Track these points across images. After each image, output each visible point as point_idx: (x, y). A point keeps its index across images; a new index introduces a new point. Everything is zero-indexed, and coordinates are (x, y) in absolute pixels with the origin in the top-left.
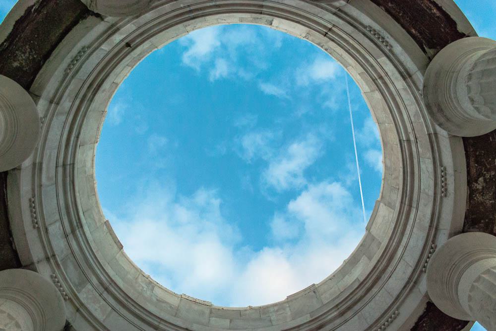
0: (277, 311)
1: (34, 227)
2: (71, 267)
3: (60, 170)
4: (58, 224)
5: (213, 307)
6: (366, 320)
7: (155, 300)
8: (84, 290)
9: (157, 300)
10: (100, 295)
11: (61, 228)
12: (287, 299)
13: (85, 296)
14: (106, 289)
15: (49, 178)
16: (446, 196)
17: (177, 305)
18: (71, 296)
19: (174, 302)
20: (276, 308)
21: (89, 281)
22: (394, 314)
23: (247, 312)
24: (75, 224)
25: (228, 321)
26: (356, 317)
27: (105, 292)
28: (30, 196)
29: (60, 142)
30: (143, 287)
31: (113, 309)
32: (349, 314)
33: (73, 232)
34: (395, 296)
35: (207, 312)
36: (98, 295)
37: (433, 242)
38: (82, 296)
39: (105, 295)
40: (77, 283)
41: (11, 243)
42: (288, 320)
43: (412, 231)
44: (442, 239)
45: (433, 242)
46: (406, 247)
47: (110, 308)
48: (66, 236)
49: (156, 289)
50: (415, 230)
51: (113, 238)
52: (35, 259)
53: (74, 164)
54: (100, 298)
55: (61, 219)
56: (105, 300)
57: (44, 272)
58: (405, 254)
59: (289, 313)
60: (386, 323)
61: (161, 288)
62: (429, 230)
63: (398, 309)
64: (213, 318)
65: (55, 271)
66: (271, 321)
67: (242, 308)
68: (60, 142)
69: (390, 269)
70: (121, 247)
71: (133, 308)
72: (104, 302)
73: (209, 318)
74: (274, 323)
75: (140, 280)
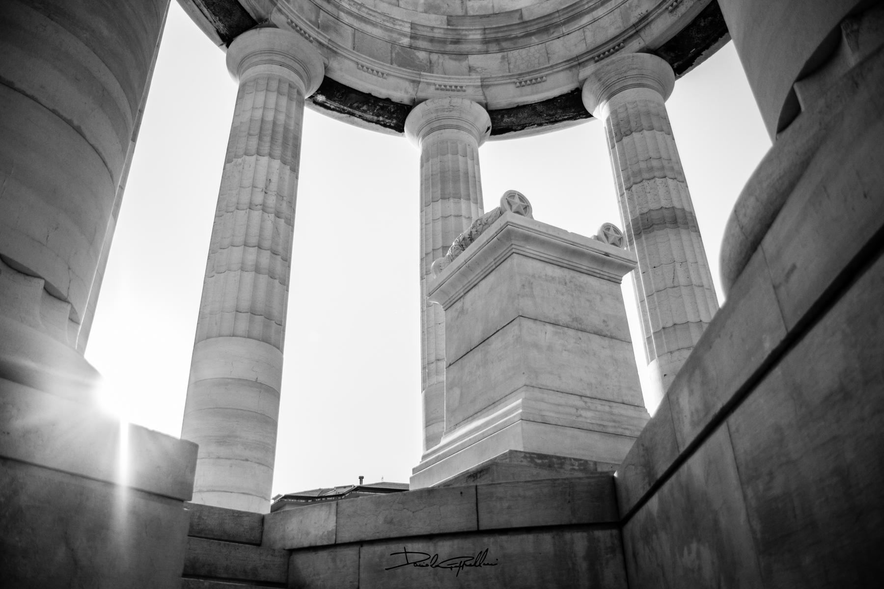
6: (509, 64)
16: (671, 12)
22: (542, 78)
26: (500, 55)
32: (493, 47)
34: (552, 63)
37: (624, 41)
42: (420, 9)
43: (612, 11)
44: (636, 44)
45: (624, 41)
46: (595, 20)
50: (617, 11)
58: (589, 27)
60: (528, 82)
62: (631, 27)
63: (546, 76)
69: (564, 29)
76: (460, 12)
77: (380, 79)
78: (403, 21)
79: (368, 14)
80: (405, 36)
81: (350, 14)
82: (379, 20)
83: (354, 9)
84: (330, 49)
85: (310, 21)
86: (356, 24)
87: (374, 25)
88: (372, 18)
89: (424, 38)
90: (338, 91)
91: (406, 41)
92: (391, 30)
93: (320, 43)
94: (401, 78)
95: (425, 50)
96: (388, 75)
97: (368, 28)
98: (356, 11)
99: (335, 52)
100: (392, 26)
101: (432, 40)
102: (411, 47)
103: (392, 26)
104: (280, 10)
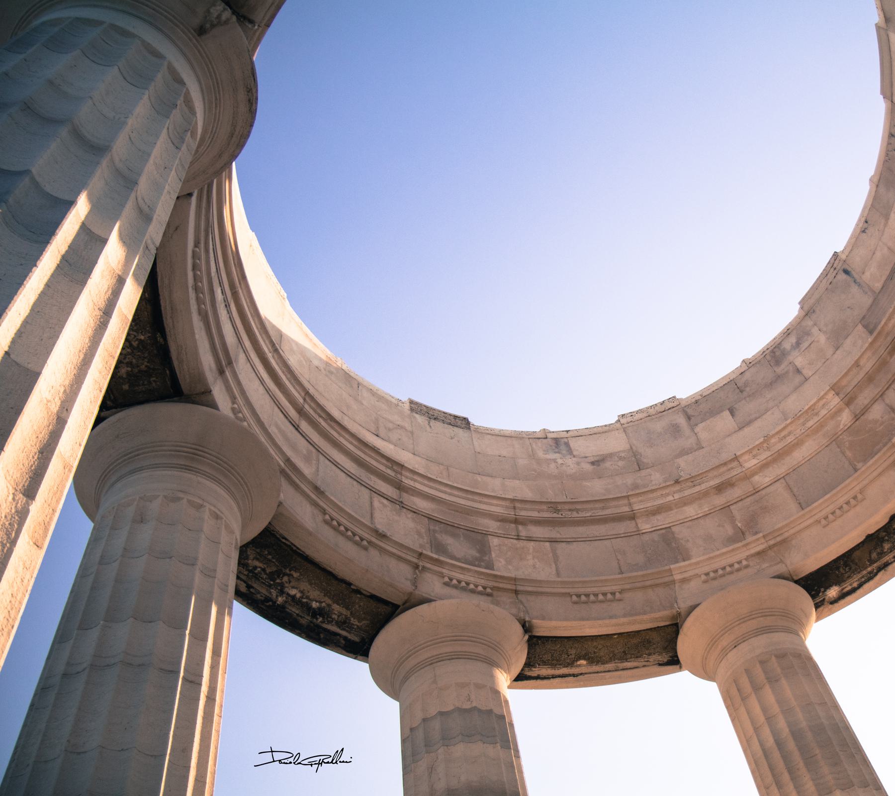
0: (798, 344)
1: (366, 549)
2: (448, 541)
3: (304, 426)
4: (377, 502)
5: (683, 404)
7: (587, 467)
8: (493, 555)
9: (593, 463)
10: (518, 538)
11: (385, 501)
12: (802, 308)
13: (503, 562)
14: (516, 521)
15: (307, 459)
17: (628, 447)
18: (491, 584)
19: (617, 444)
20: (793, 339)
21: (486, 534)
23: (747, 375)
24: (389, 472)
25: (727, 413)
27: (520, 527)
28: (320, 518)
29: (268, 390)
30: (555, 461)
31: (552, 541)
33: (399, 486)
35: (681, 420)
36: (515, 541)
38: (502, 567)
39: (523, 532)
40: (478, 555)
41: (358, 591)
42: (830, 352)
47: (548, 544)
48: (402, 505)
49: (573, 444)
51: (443, 422)
52: (408, 586)
53: (307, 393)
54: (521, 544)
55: (371, 490)
56: (529, 539)
57: (431, 585)
59: (822, 338)
61: (579, 435)
64: (701, 426)
65: (442, 573)
66: (798, 371)
67: (733, 372)
68: (268, 390)
70: (464, 423)
71: (575, 514)
72: (532, 543)
73: (693, 430)
74: (807, 372)
75: (541, 454)
76: (867, 301)
77: (858, 508)
78: (822, 398)
79: (781, 440)
80: (839, 411)
81: (764, 466)
82: (798, 432)
83: (765, 455)
84: (774, 545)
85: (732, 540)
86: (779, 470)
87: (798, 443)
88: (790, 439)
89: (860, 387)
90: (838, 568)
91: (846, 418)
92: (821, 425)
93: (759, 554)
94: (880, 475)
95: (874, 401)
96: (861, 491)
97: (799, 455)
98: (768, 454)
99: (784, 541)
100: (816, 419)
101: (870, 379)
102: (857, 418)
103: (816, 419)
104: (684, 581)
